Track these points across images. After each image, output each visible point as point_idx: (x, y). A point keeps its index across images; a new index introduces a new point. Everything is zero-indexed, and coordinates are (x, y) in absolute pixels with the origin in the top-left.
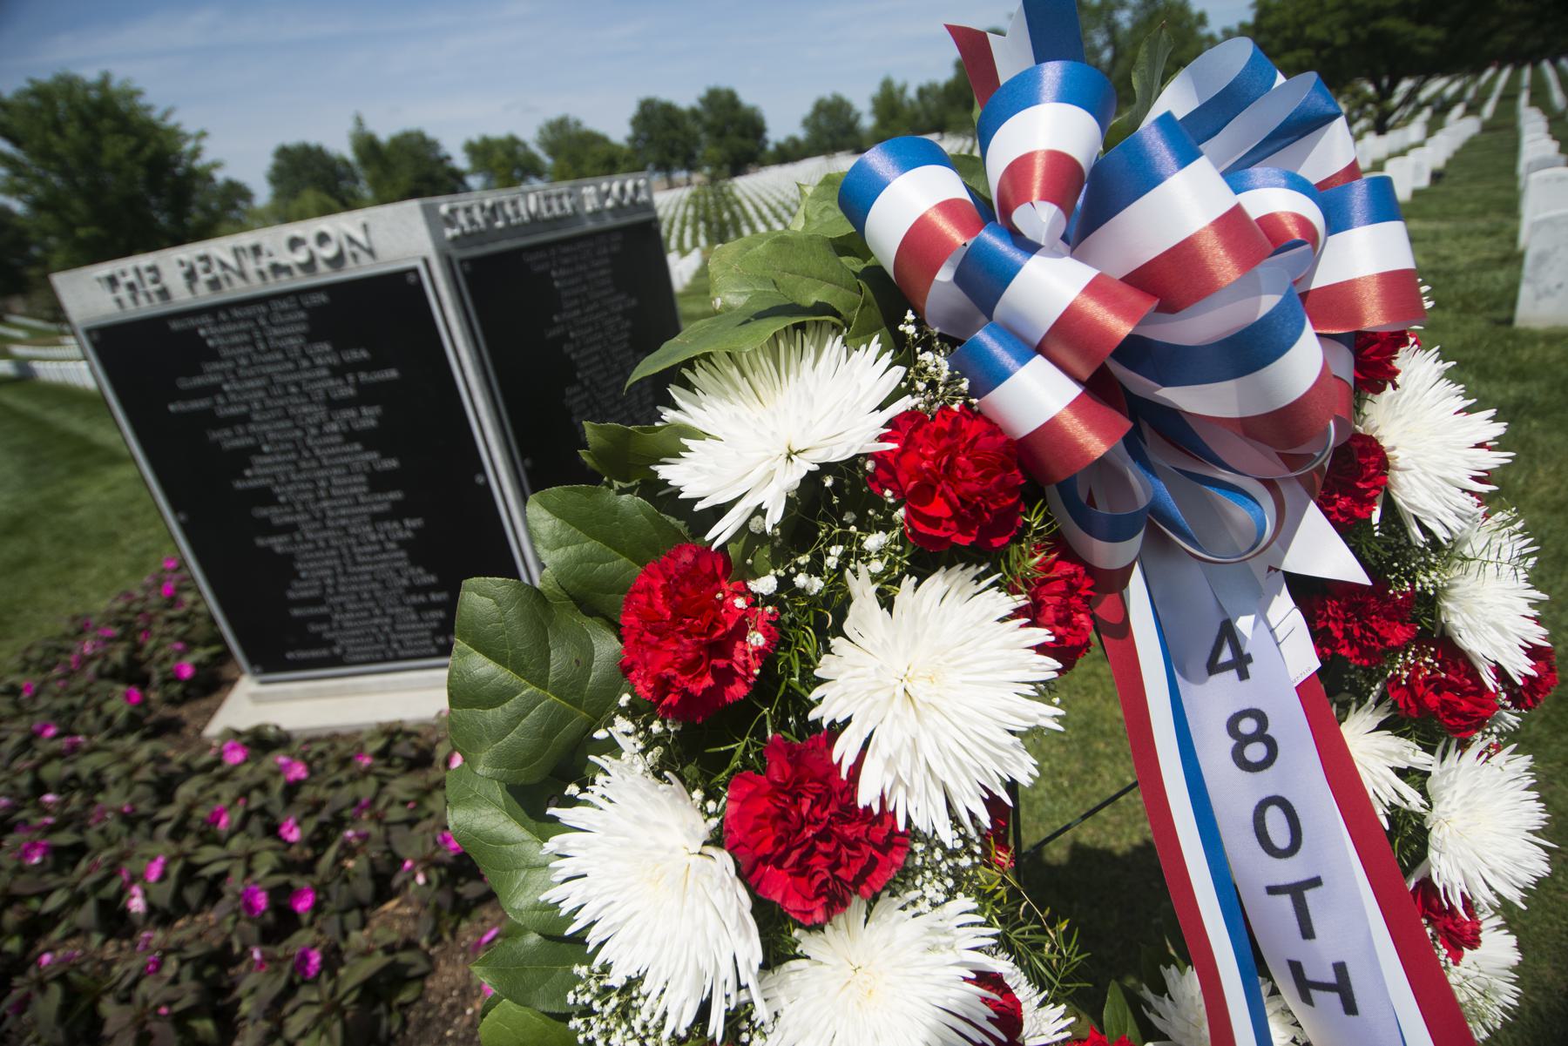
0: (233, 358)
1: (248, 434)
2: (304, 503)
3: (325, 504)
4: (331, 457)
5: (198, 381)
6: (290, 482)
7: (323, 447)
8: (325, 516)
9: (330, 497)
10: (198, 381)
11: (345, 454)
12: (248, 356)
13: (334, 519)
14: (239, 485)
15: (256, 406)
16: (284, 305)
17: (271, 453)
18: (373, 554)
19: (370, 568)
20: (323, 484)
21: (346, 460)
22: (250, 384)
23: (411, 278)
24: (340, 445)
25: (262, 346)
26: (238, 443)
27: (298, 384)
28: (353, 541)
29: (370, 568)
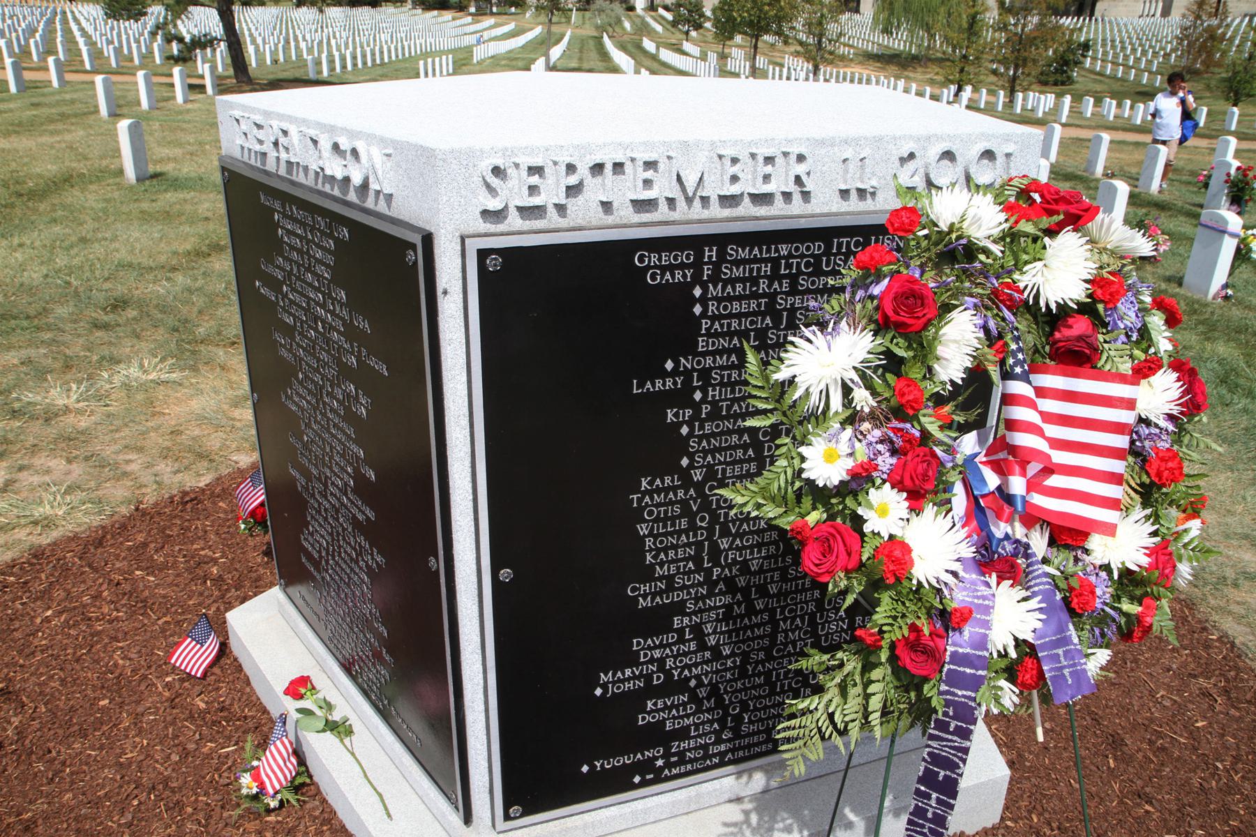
23: (493, 263)
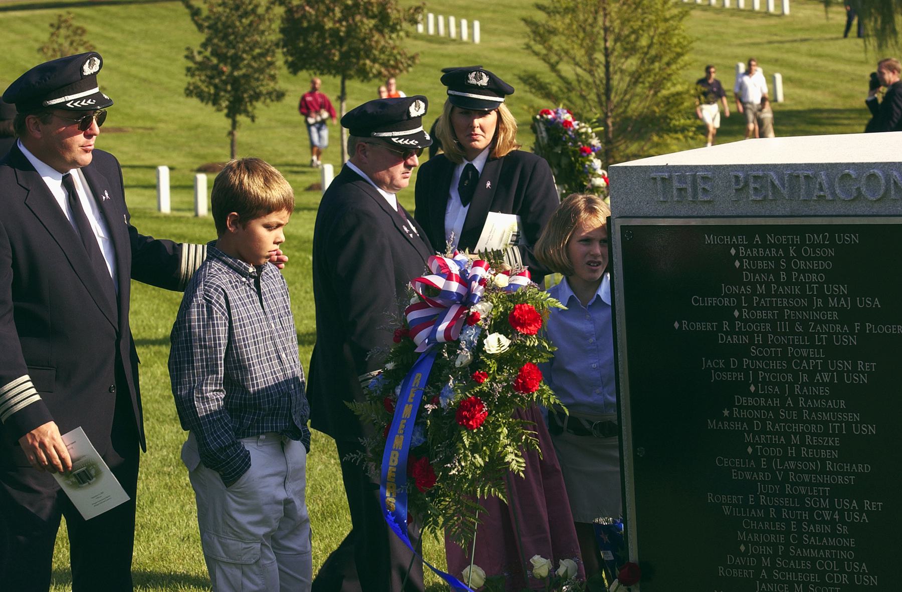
0: (753, 285)
1: (740, 369)
2: (769, 459)
3: (792, 465)
4: (811, 410)
5: (711, 301)
6: (764, 431)
7: (807, 398)
8: (786, 479)
9: (798, 458)
10: (711, 301)
11: (827, 410)
12: (768, 285)
13: (793, 484)
14: (712, 425)
15: (758, 339)
16: (818, 239)
17: (756, 394)
18: (821, 536)
19: (814, 553)
20: (796, 440)
21: (826, 417)
22: (759, 314)
24: (827, 398)
25: (783, 275)
26: (727, 376)
27: (805, 323)
28: (806, 515)
29: (814, 553)
